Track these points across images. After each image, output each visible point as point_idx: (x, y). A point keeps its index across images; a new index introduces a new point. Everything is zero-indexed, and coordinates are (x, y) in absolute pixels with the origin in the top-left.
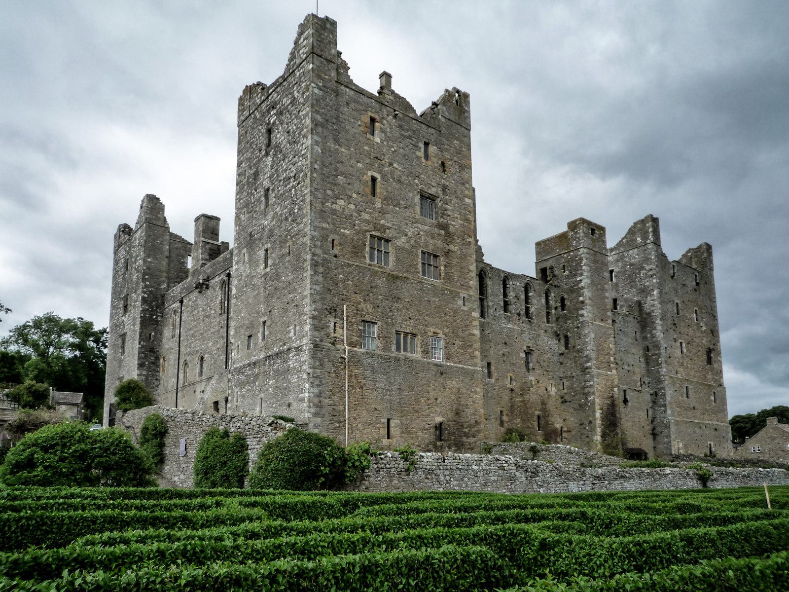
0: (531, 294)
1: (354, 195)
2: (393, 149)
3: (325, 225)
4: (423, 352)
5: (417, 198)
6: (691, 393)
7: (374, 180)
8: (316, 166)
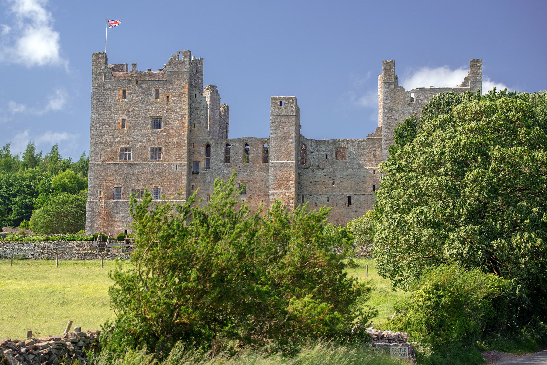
5: (149, 122)
7: (124, 120)
8: (93, 124)
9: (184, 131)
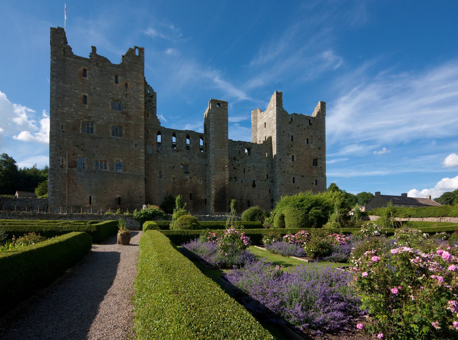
1: (74, 105)
2: (96, 81)
4: (110, 168)
6: (296, 181)
8: (54, 95)
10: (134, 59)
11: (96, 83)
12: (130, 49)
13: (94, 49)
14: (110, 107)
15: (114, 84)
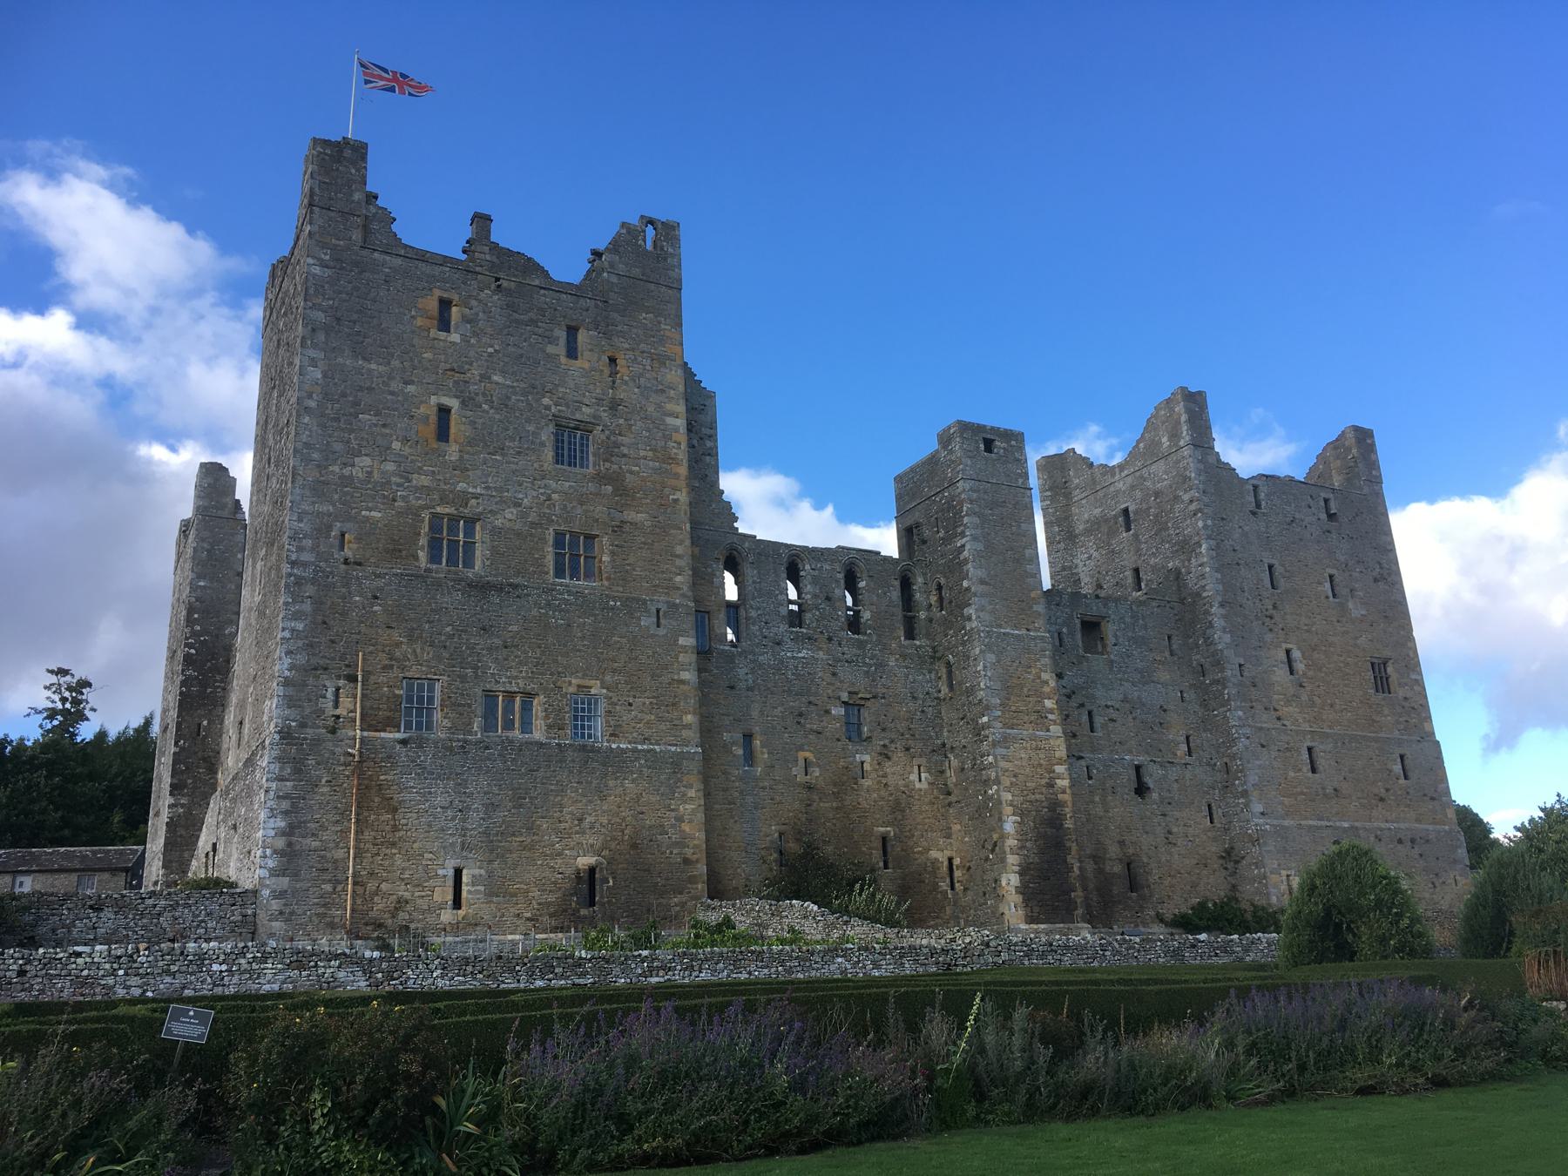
0: (862, 584)
1: (396, 445)
3: (326, 508)
4: (549, 727)
5: (547, 435)
6: (1321, 763)
7: (444, 412)
9: (675, 489)
10: (641, 272)
11: (490, 355)
12: (623, 225)
13: (482, 221)
14: (549, 454)
15: (563, 360)
